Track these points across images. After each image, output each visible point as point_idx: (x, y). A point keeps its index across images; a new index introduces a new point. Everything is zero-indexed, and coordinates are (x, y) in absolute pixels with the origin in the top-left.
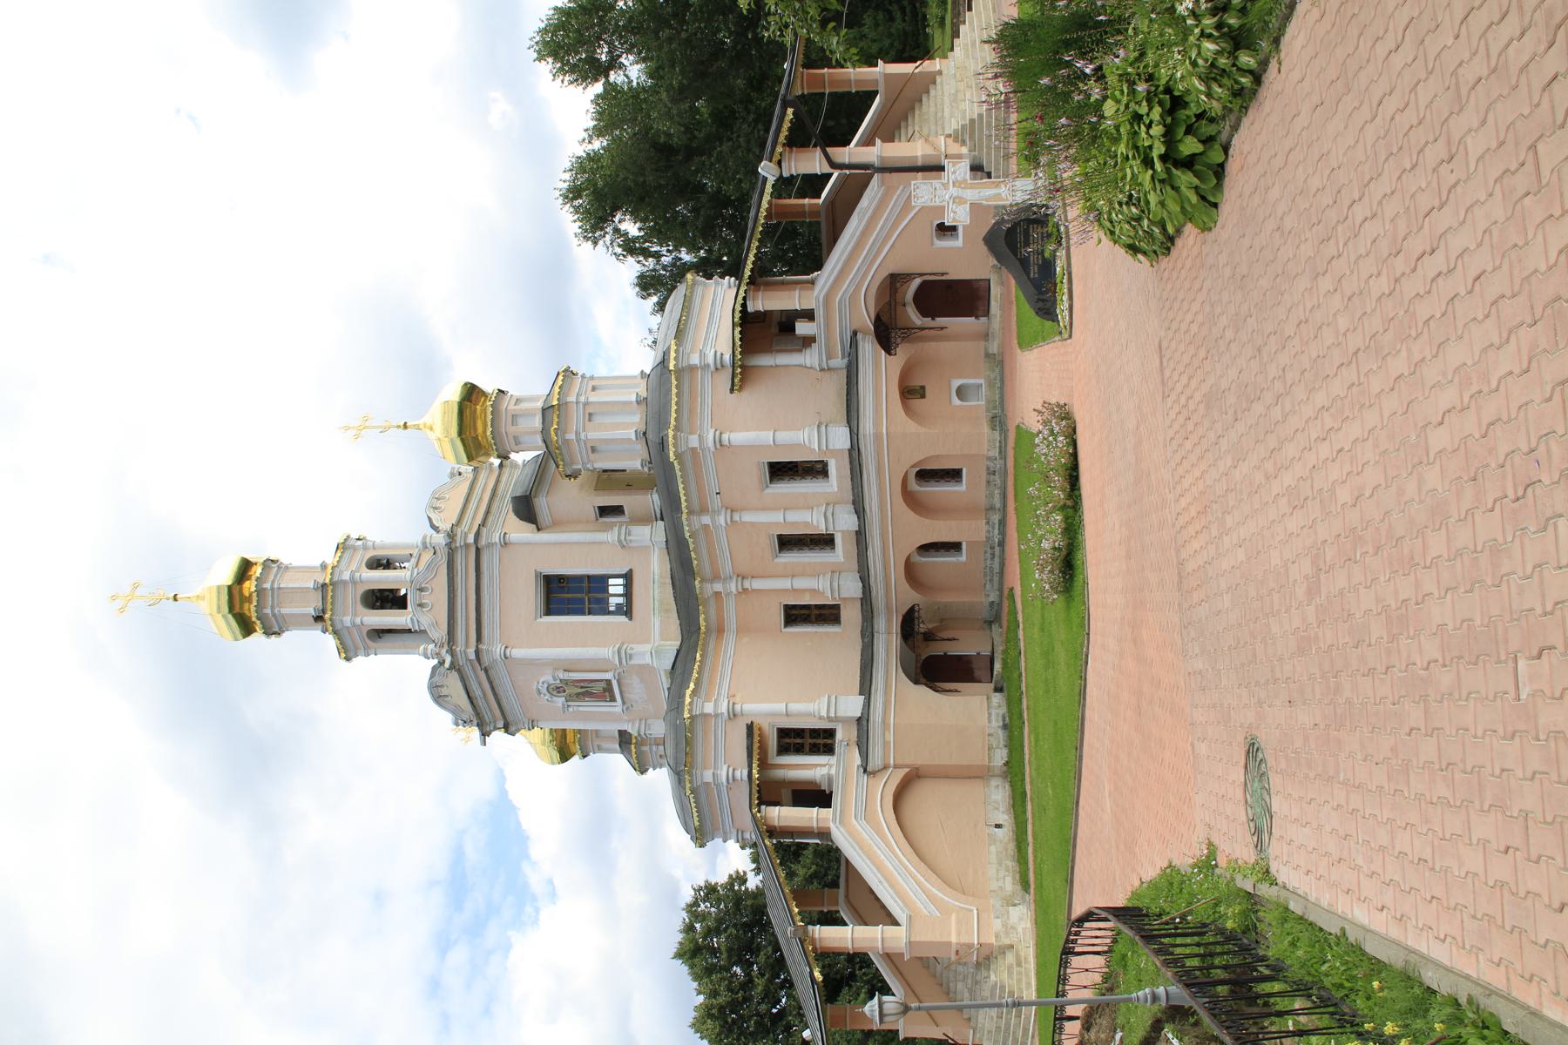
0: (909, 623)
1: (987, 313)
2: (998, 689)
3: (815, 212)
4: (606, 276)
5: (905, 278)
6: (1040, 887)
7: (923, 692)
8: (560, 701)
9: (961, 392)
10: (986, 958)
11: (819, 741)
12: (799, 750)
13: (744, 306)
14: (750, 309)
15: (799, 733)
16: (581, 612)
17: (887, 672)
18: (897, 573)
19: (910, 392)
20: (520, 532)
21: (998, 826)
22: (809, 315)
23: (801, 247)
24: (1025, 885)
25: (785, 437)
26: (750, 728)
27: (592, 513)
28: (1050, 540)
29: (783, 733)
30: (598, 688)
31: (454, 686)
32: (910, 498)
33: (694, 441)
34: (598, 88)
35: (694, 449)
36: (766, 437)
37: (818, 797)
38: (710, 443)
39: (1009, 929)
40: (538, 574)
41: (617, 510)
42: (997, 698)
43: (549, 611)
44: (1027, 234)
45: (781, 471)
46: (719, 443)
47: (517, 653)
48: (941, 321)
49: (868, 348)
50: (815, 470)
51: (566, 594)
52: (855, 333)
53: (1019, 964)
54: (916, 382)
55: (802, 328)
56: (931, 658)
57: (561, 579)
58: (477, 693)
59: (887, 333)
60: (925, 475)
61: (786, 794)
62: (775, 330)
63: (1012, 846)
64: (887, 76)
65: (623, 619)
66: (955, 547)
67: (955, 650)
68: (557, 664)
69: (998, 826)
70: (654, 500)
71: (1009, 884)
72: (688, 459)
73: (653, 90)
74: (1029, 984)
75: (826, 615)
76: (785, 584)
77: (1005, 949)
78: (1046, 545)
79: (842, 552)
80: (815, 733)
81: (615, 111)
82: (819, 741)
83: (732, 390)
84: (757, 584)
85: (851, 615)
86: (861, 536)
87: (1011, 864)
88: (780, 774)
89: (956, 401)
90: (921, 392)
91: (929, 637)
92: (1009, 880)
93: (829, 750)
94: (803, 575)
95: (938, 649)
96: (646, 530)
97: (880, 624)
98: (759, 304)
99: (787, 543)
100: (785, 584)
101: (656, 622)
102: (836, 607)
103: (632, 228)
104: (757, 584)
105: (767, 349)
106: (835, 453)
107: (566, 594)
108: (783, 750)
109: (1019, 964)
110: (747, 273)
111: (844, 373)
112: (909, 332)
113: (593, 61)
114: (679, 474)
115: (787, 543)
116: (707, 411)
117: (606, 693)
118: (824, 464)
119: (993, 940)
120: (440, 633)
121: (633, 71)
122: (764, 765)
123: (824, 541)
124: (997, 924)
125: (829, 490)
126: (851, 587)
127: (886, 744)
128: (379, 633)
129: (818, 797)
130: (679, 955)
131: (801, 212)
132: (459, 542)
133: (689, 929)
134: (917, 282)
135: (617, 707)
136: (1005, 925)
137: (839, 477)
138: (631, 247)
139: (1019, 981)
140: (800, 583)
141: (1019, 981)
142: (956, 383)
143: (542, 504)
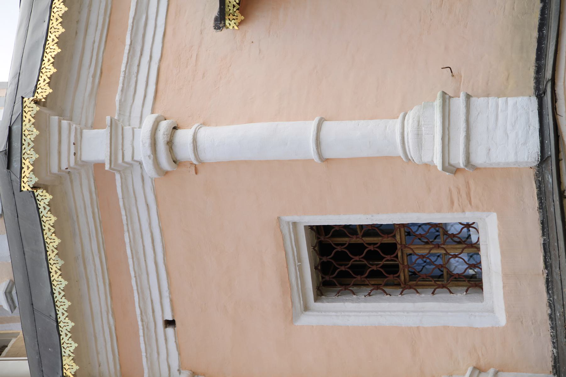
25: (350, 135)
33: (96, 146)
35: (99, 166)
36: (294, 135)
38: (142, 151)
45: (352, 260)
46: (172, 163)
72: (83, 194)
83: (220, 21)
114: (53, 241)
116: (146, 73)
118: (465, 241)
125: (481, 321)
137: (511, 276)
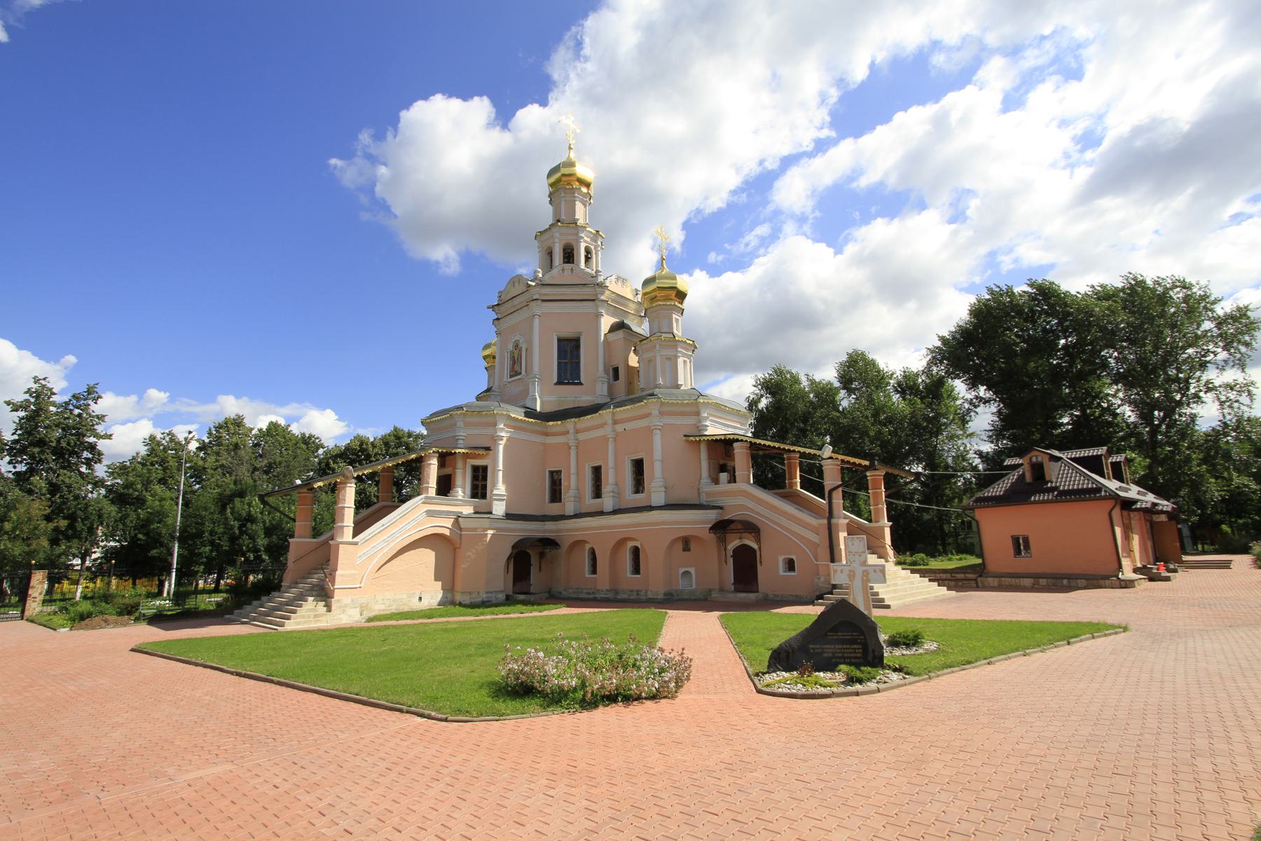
0: (548, 543)
1: (737, 590)
2: (508, 597)
3: (792, 485)
4: (739, 388)
5: (758, 541)
6: (369, 628)
7: (508, 551)
8: (511, 347)
9: (687, 573)
10: (324, 594)
11: (479, 489)
12: (475, 478)
13: (737, 440)
14: (735, 445)
15: (485, 478)
16: (559, 358)
17: (520, 530)
18: (578, 535)
19: (686, 543)
20: (607, 322)
21: (420, 599)
22: (733, 479)
23: (770, 475)
24: (370, 620)
26: (488, 449)
27: (615, 363)
28: (558, 673)
29: (485, 469)
30: (517, 368)
31: (519, 289)
32: (622, 542)
34: (837, 384)
36: (658, 454)
37: (445, 487)
39: (343, 609)
40: (580, 333)
41: (616, 377)
42: (502, 597)
43: (559, 340)
44: (853, 642)
47: (536, 321)
48: (731, 561)
49: (712, 516)
50: (639, 485)
51: (569, 349)
52: (721, 508)
53: (316, 616)
54: (692, 546)
55: (724, 476)
56: (529, 556)
57: (578, 347)
58: (516, 301)
59: (722, 528)
60: (636, 552)
61: (447, 471)
62: (722, 462)
63: (406, 609)
64: (882, 528)
65: (555, 380)
66: (594, 571)
67: (534, 570)
68: (530, 343)
69: (420, 599)
70: (622, 396)
71: (379, 608)
73: (838, 411)
74: (299, 623)
75: (556, 495)
76: (573, 470)
77: (329, 607)
78: (551, 669)
79: (590, 503)
80: (485, 487)
81: (825, 395)
82: (479, 489)
84: (573, 452)
85: (554, 509)
86: (601, 513)
87: (393, 609)
88: (460, 464)
89: (682, 570)
90: (686, 548)
91: (542, 555)
92: (382, 607)
93: (474, 495)
94: (578, 480)
95: (534, 560)
96: (605, 392)
97: (550, 525)
98: (740, 452)
99: (597, 471)
100: (573, 470)
101: (553, 398)
102: (560, 501)
103: (763, 403)
104: (573, 452)
105: (711, 457)
106: (649, 496)
107: (569, 349)
108: (476, 469)
109: (316, 616)
110: (758, 441)
111: (697, 502)
112: (723, 541)
113: (851, 381)
115: (597, 471)
117: (515, 373)
119: (336, 597)
120: (547, 280)
121: (845, 401)
122: (466, 456)
123: (597, 493)
124: (347, 600)
126: (569, 508)
127: (475, 529)
128: (551, 254)
129: (445, 487)
130: (396, 429)
131: (792, 477)
132: (599, 290)
133: (410, 435)
134: (755, 546)
135: (506, 379)
136: (346, 606)
138: (752, 404)
139: (303, 617)
140: (573, 478)
141: (303, 617)
142: (692, 570)
143: (620, 334)
